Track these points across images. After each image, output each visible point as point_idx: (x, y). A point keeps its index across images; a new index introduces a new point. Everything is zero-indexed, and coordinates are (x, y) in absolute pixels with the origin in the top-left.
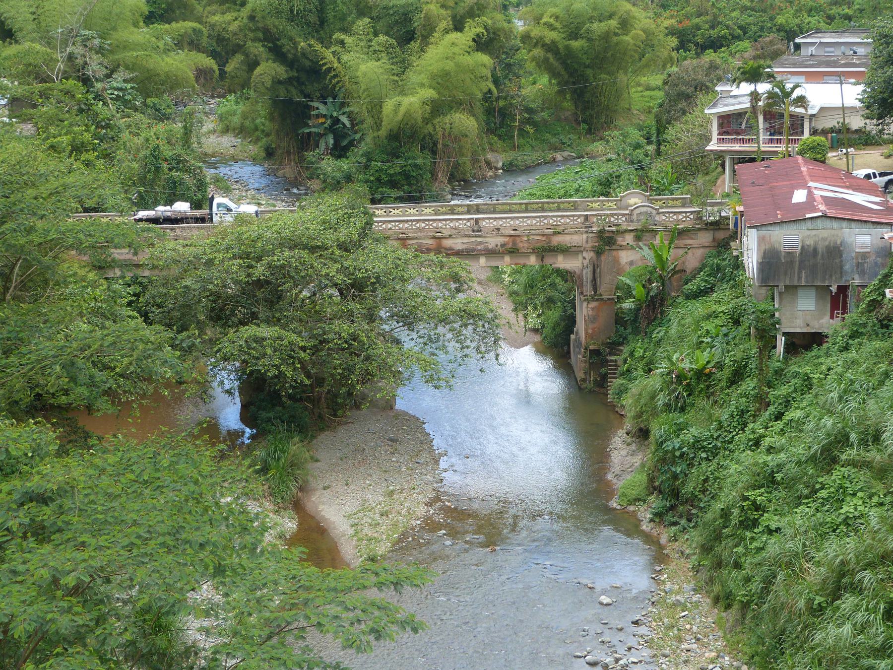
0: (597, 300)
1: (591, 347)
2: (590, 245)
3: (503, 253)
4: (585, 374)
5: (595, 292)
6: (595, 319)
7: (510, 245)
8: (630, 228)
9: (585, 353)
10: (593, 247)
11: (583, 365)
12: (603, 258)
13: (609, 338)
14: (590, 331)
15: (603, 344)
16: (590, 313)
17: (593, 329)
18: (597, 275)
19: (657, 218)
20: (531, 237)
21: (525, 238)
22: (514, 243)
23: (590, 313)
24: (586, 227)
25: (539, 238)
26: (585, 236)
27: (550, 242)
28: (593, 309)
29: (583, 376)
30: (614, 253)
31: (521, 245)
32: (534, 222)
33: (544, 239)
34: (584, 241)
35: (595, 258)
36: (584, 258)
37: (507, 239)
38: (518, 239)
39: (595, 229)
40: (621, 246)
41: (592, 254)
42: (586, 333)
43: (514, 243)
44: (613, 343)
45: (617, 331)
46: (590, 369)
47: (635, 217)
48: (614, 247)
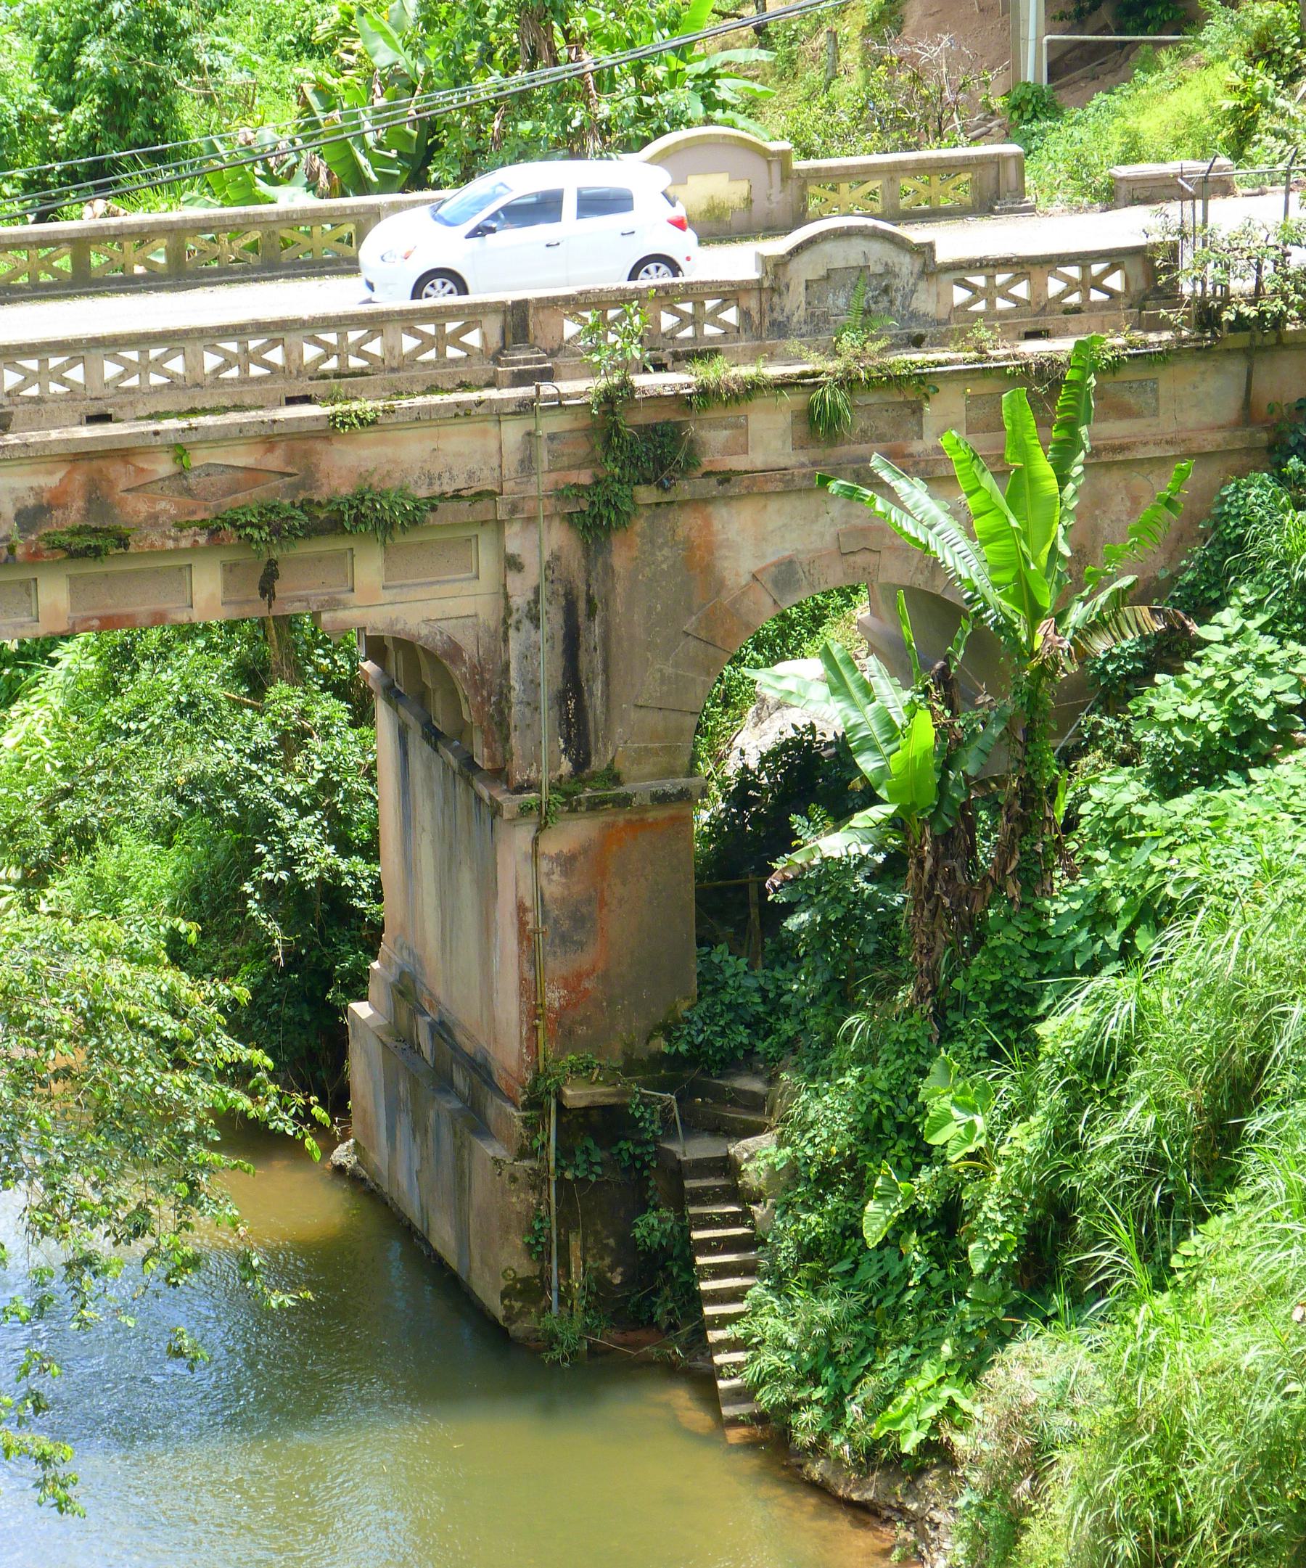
0: (595, 806)
1: (576, 1095)
2: (545, 481)
3: (34, 558)
4: (537, 1250)
5: (581, 764)
6: (579, 920)
7: (73, 515)
8: (774, 371)
9: (532, 1127)
10: (560, 494)
11: (521, 1200)
12: (620, 558)
13: (667, 1031)
14: (554, 996)
15: (631, 1066)
16: (554, 887)
17: (572, 983)
18: (590, 662)
19: (925, 302)
20: (199, 458)
21: (164, 467)
22: (97, 497)
23: (554, 887)
24: (521, 379)
25: (242, 457)
26: (512, 432)
27: (308, 478)
28: (567, 862)
29: (523, 1267)
30: (687, 523)
31: (139, 507)
32: (211, 361)
33: (275, 461)
34: (511, 461)
35: (574, 561)
36: (513, 563)
37: (50, 480)
38: (121, 476)
39: (574, 387)
40: (726, 477)
41: (557, 537)
42: (534, 1012)
43: (97, 497)
44: (696, 1057)
45: (711, 982)
46: (566, 1222)
47: (795, 302)
48: (684, 489)
